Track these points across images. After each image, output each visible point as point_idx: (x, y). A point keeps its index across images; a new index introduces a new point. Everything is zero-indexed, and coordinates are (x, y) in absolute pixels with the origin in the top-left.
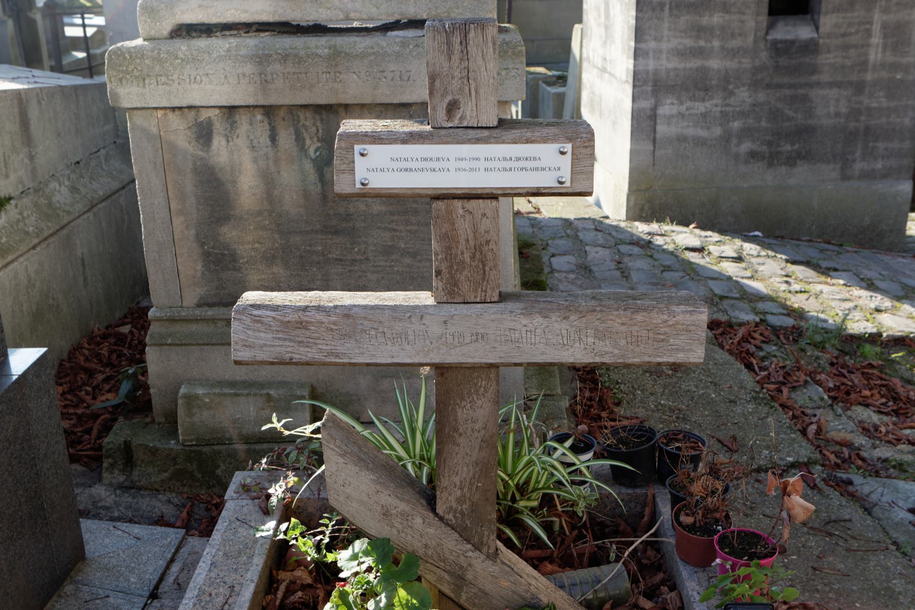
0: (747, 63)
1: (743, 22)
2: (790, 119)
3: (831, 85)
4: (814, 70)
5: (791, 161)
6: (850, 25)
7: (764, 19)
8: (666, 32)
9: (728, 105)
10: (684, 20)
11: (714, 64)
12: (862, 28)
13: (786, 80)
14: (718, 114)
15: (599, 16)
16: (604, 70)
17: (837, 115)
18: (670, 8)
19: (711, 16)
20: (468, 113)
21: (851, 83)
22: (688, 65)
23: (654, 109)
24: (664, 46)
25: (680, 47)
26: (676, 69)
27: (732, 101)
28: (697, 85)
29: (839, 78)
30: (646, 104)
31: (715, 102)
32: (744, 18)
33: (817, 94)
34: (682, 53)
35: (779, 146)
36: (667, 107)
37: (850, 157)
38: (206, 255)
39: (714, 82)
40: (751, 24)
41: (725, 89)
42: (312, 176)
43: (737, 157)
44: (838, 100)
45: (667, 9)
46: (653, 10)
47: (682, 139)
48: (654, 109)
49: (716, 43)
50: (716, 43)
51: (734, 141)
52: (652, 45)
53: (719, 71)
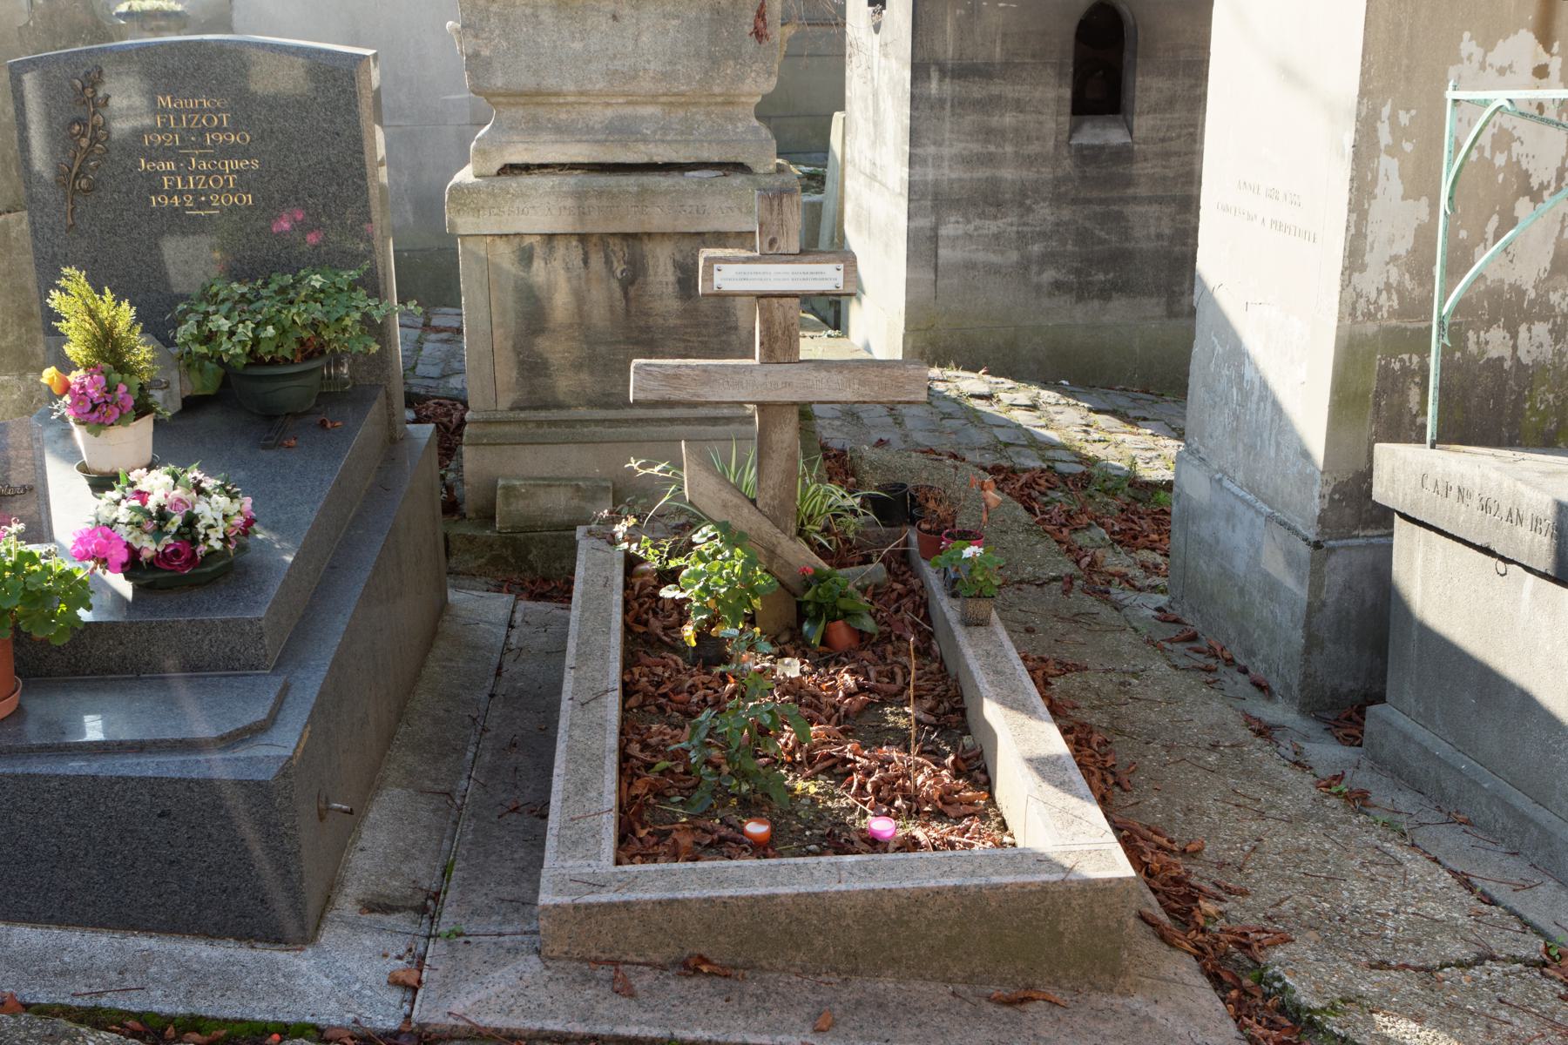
0: (1047, 173)
1: (1041, 123)
2: (1102, 242)
3: (1151, 200)
4: (1129, 182)
5: (1105, 293)
6: (1169, 128)
7: (1066, 120)
8: (947, 135)
9: (1025, 224)
10: (970, 119)
11: (1008, 174)
12: (1185, 132)
13: (1095, 194)
14: (1014, 236)
15: (866, 108)
16: (873, 177)
17: (1159, 236)
18: (952, 106)
19: (1002, 115)
21: (1174, 199)
22: (975, 175)
23: (935, 229)
24: (946, 151)
25: (965, 153)
26: (960, 180)
27: (1030, 219)
28: (988, 199)
29: (1160, 192)
30: (925, 222)
31: (1009, 220)
32: (1042, 118)
33: (1131, 210)
34: (967, 161)
35: (1089, 274)
36: (951, 226)
37: (1176, 289)
38: (521, 363)
39: (1007, 196)
40: (1051, 125)
41: (1021, 204)
42: (618, 293)
43: (1038, 288)
44: (1159, 219)
46: (932, 108)
47: (970, 266)
48: (935, 229)
49: (1009, 149)
50: (1009, 149)
51: (1034, 268)
52: (931, 150)
53: (1014, 182)
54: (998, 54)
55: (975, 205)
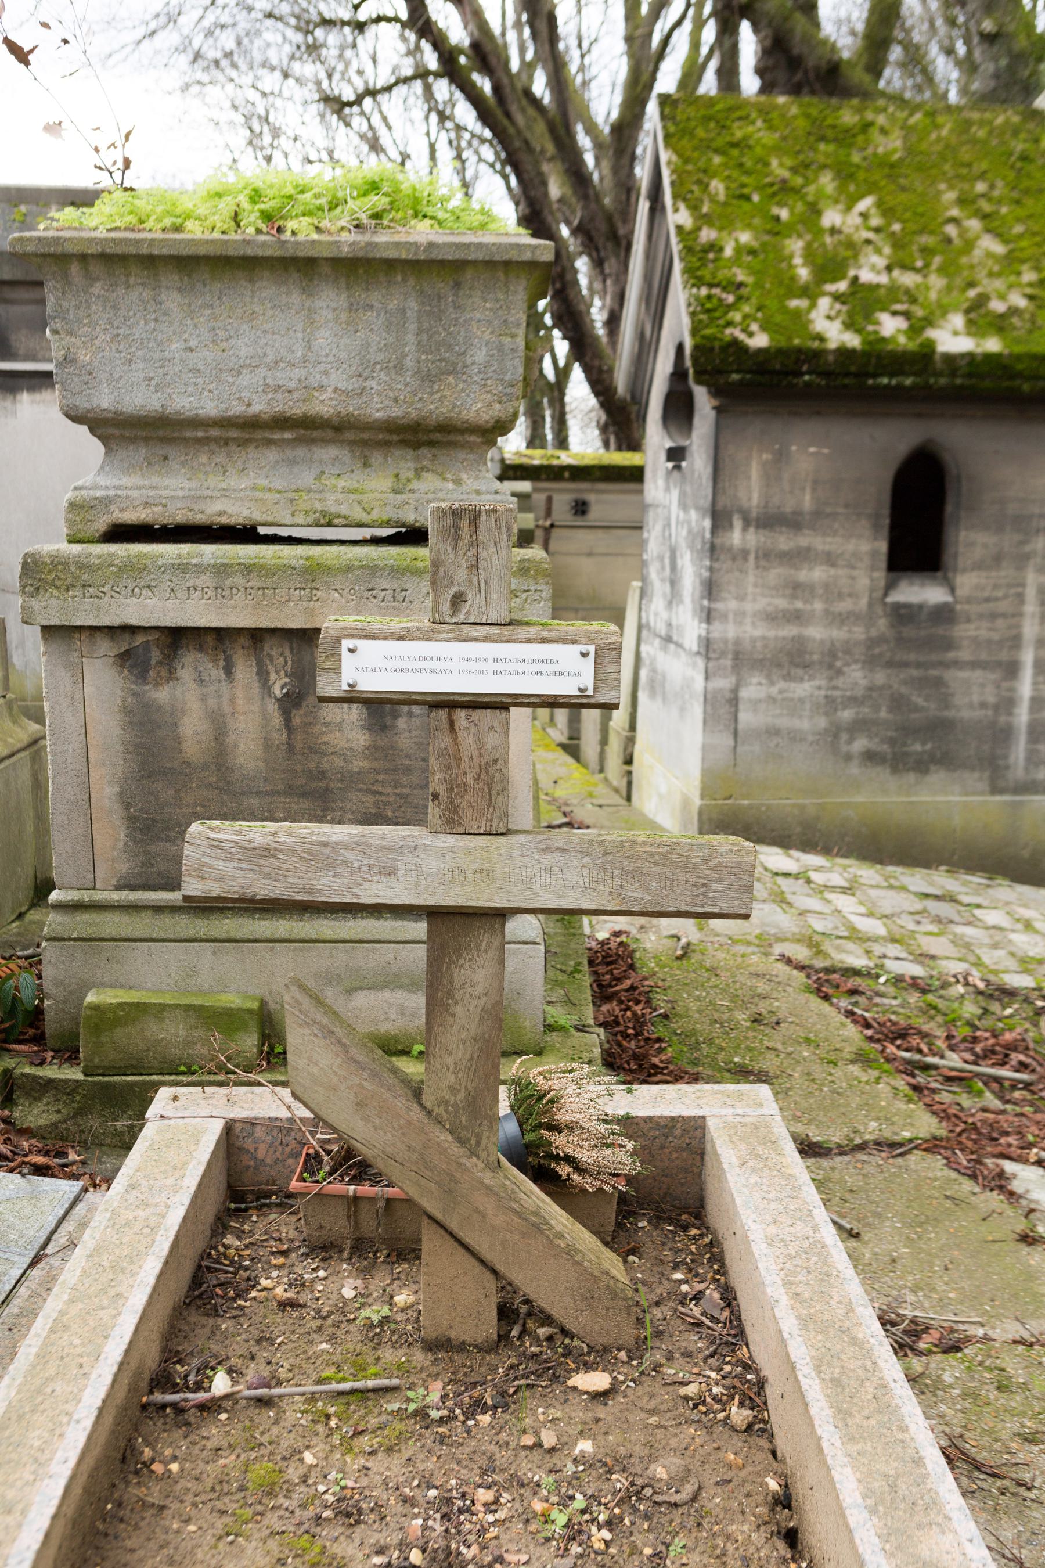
0: (859, 633)
1: (853, 578)
2: (917, 709)
3: (975, 665)
4: (949, 644)
5: (921, 766)
6: (996, 587)
7: (881, 575)
8: (750, 589)
9: (835, 688)
10: (776, 573)
11: (816, 632)
12: (1012, 591)
13: (912, 657)
14: (822, 701)
15: (663, 568)
16: (668, 639)
17: (983, 705)
18: (757, 558)
19: (811, 569)
20: (472, 609)
21: (999, 664)
23: (735, 691)
24: (749, 607)
25: (770, 609)
26: (764, 638)
27: (840, 682)
28: (792, 659)
29: (984, 656)
30: (723, 683)
31: (817, 683)
32: (855, 573)
33: (955, 677)
34: (772, 618)
35: (905, 744)
36: (752, 688)
37: (1001, 762)
38: (131, 819)
39: (816, 657)
40: (863, 582)
41: (830, 666)
42: (277, 720)
43: (848, 757)
44: (983, 686)
45: (752, 558)
46: (734, 559)
47: (773, 732)
48: (735, 691)
49: (818, 606)
50: (818, 606)
51: (844, 736)
52: (733, 605)
53: (822, 642)
54: (807, 502)
55: (779, 666)
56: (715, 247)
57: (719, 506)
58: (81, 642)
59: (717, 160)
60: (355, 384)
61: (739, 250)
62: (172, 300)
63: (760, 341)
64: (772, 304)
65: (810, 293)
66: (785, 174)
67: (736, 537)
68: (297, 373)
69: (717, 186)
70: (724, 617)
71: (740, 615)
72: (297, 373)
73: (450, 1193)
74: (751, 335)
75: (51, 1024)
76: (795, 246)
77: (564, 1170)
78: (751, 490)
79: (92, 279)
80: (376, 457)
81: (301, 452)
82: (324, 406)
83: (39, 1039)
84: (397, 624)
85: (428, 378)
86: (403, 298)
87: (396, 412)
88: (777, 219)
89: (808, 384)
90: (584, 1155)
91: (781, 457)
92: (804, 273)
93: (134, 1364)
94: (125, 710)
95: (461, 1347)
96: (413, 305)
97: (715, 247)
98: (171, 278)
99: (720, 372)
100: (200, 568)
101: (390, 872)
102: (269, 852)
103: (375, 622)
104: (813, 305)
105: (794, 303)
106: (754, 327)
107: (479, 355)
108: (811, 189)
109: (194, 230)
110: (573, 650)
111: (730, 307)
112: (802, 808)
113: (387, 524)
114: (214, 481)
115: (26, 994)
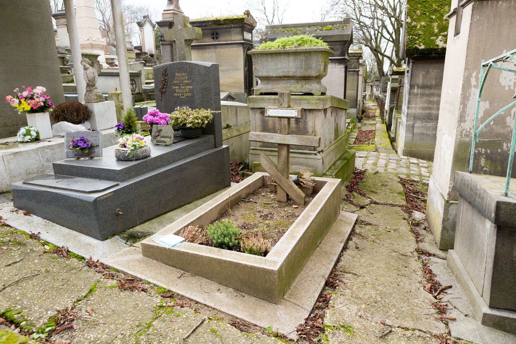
10: (425, 99)
20: (283, 106)
22: (425, 112)
23: (414, 124)
30: (411, 123)
34: (423, 108)
45: (419, 95)
47: (422, 134)
48: (414, 124)
52: (414, 105)
54: (434, 82)
55: (424, 119)
56: (415, 26)
57: (412, 84)
58: (255, 110)
59: (419, 6)
60: (295, 71)
61: (421, 27)
62: (269, 59)
63: (422, 47)
64: (427, 39)
65: (437, 35)
66: (436, 7)
67: (416, 91)
68: (287, 69)
69: (418, 12)
70: (412, 108)
71: (416, 108)
72: (287, 69)
73: (280, 181)
74: (420, 46)
75: (250, 167)
76: (435, 24)
77: (302, 184)
78: (420, 80)
79: (259, 57)
80: (299, 82)
81: (288, 81)
82: (291, 74)
83: (248, 169)
84: (274, 107)
85: (306, 69)
86: (302, 57)
87: (301, 75)
88: (432, 18)
89: (434, 56)
90: (305, 182)
91: (428, 72)
92: (436, 31)
93: (240, 194)
94: (261, 120)
95: (282, 202)
96: (304, 58)
97: (415, 26)
98: (269, 56)
99: (412, 55)
100: (272, 99)
101: (273, 138)
102: (259, 135)
103: (272, 107)
104: (437, 38)
105: (432, 38)
106: (421, 44)
107: (314, 65)
108: (442, 11)
109: (273, 49)
110: (295, 111)
111: (416, 40)
112: (428, 151)
113: (300, 92)
114: (275, 86)
115: (247, 162)
